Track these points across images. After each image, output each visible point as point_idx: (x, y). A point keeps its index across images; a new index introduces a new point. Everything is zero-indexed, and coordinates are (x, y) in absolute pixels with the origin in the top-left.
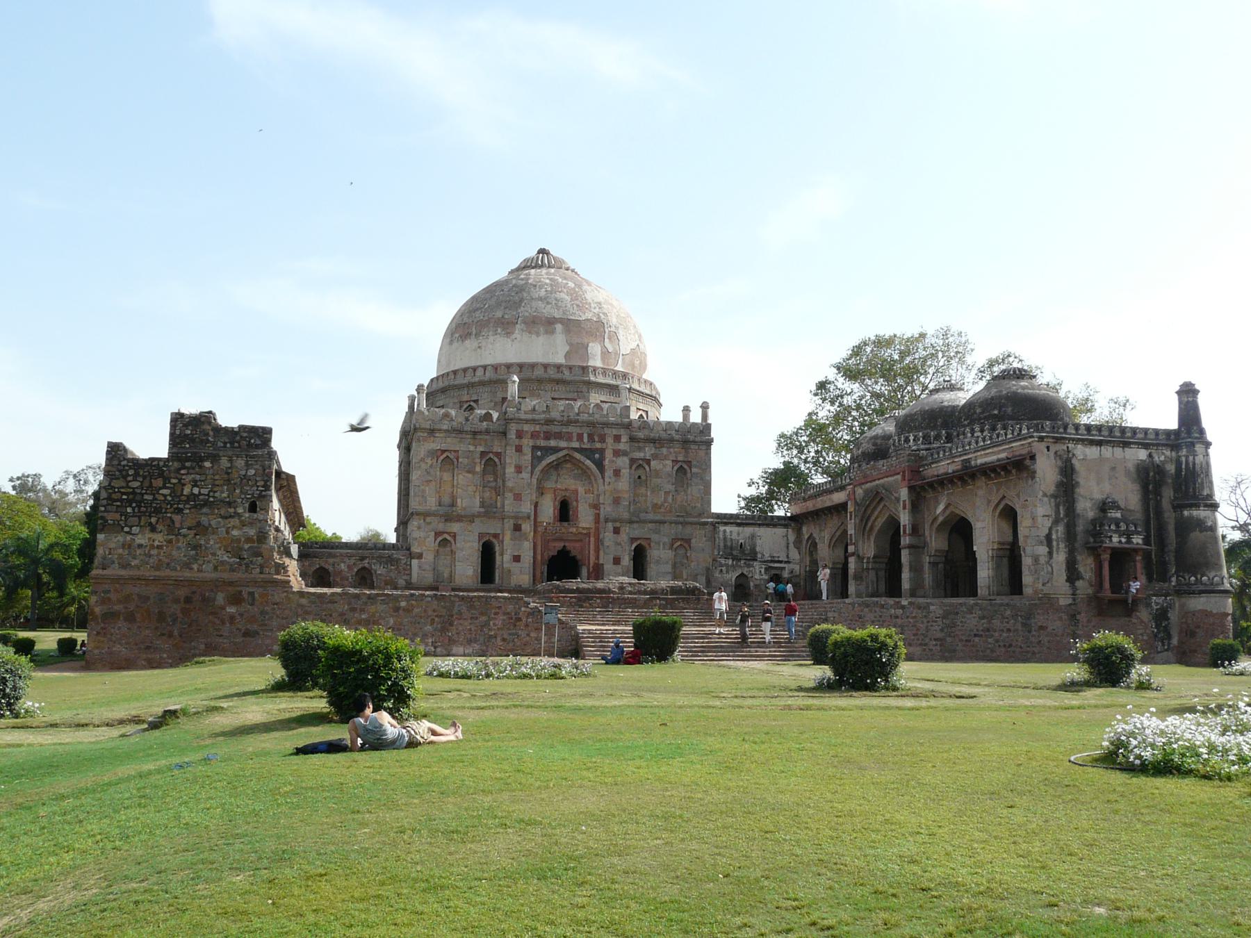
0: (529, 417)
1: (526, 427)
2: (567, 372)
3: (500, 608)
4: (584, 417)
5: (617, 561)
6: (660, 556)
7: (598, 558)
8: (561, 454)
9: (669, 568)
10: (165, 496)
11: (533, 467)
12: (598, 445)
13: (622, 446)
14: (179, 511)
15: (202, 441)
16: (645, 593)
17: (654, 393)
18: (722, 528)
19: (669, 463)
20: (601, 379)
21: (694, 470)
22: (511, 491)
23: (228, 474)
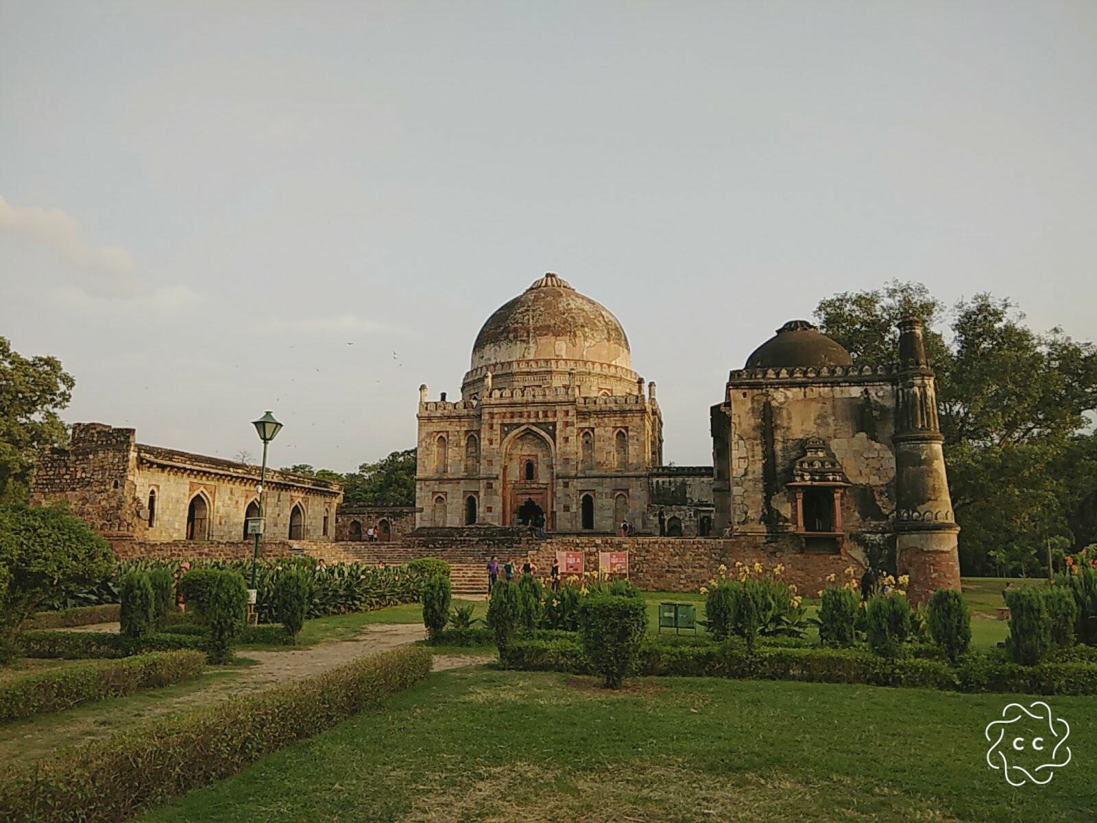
0: (498, 402)
1: (496, 410)
2: (534, 365)
3: (271, 551)
4: (539, 399)
5: (567, 508)
6: (604, 506)
7: (552, 507)
8: (522, 428)
9: (610, 513)
10: (66, 480)
11: (502, 440)
12: (551, 420)
13: (569, 419)
14: (74, 490)
15: (89, 441)
16: (480, 535)
17: (618, 375)
18: (655, 480)
19: (611, 429)
20: (562, 366)
21: (630, 433)
22: (485, 458)
23: (102, 462)
